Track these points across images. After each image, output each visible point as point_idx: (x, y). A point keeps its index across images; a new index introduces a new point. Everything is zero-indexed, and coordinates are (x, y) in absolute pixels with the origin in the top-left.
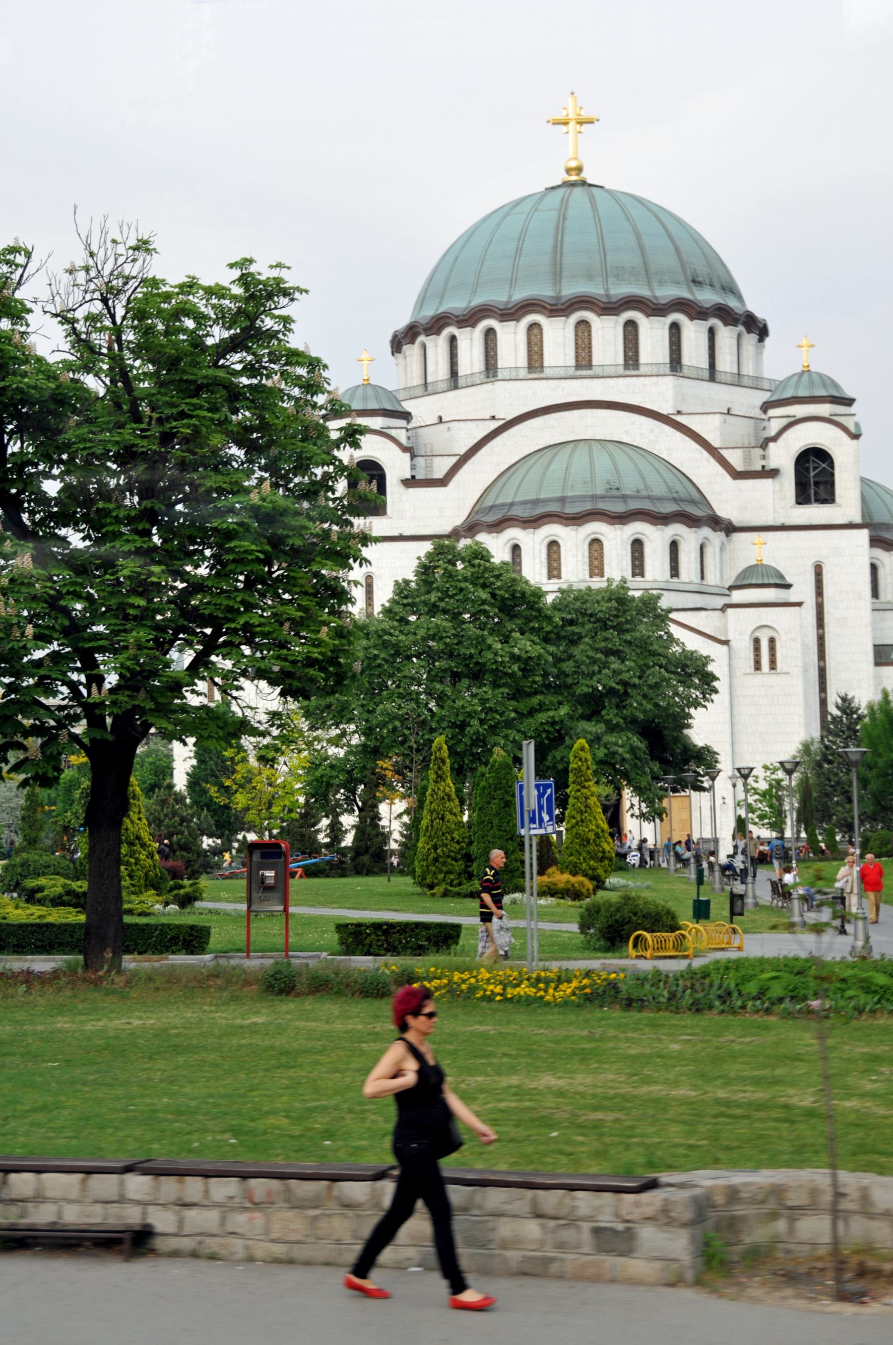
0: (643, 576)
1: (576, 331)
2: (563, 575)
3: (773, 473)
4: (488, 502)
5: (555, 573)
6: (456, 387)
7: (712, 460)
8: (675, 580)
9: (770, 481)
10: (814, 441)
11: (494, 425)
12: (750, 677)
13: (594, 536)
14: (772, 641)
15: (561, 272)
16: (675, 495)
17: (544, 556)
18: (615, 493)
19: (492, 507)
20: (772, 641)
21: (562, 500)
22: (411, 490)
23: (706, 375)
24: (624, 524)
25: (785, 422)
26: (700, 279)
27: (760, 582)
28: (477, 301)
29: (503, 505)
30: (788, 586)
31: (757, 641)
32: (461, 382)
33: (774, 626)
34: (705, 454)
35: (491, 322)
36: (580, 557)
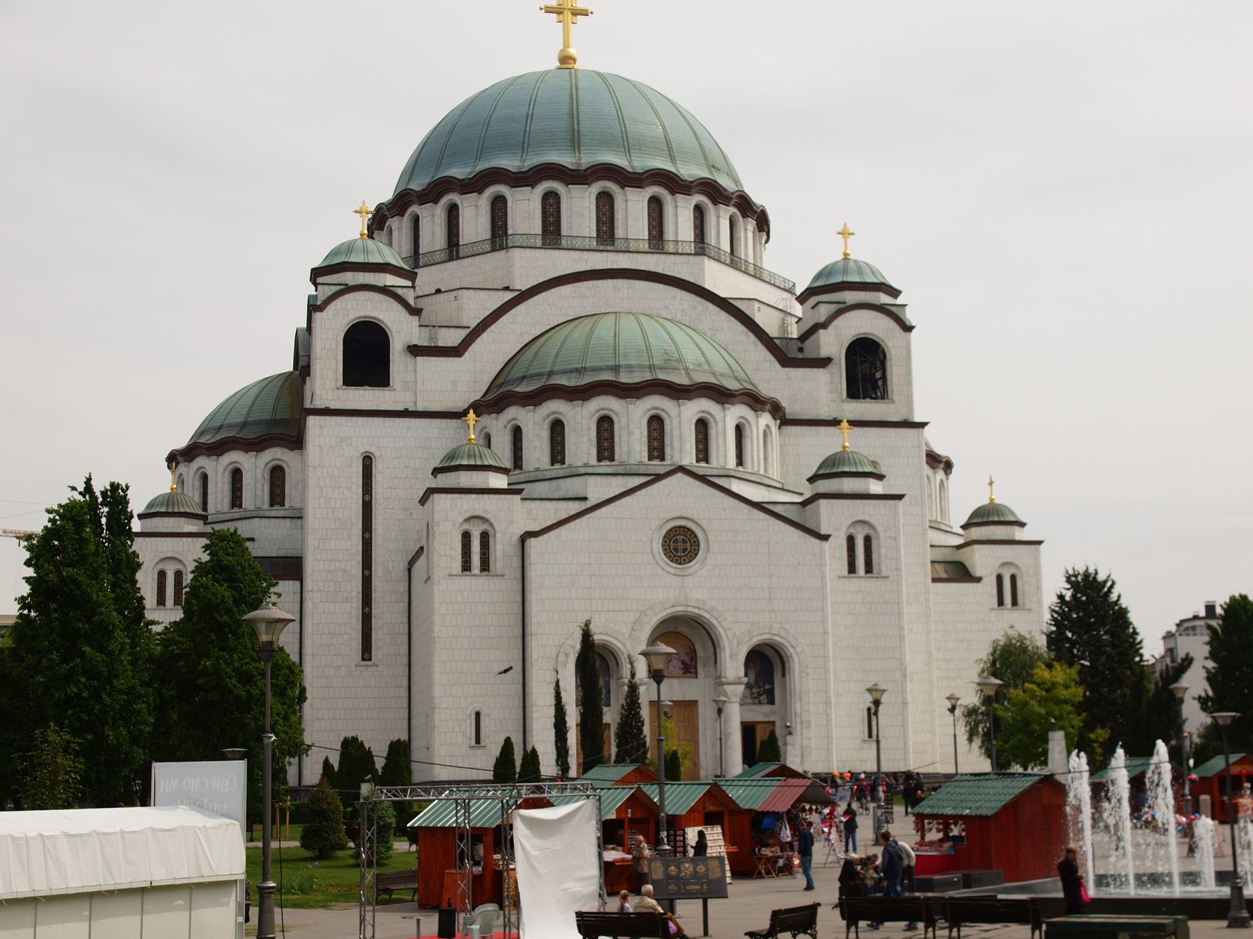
0: (707, 460)
1: (597, 203)
2: (617, 457)
3: (824, 362)
4: (518, 371)
5: (606, 454)
6: (458, 258)
7: (759, 344)
8: (740, 468)
10: (866, 331)
11: (508, 296)
13: (654, 412)
14: (868, 540)
16: (736, 373)
17: (594, 433)
18: (674, 364)
19: (524, 377)
20: (868, 540)
22: (418, 358)
24: (689, 399)
25: (834, 308)
26: (720, 167)
27: (853, 470)
28: (482, 166)
29: (540, 375)
30: (880, 477)
33: (873, 521)
34: (752, 337)
35: (501, 189)
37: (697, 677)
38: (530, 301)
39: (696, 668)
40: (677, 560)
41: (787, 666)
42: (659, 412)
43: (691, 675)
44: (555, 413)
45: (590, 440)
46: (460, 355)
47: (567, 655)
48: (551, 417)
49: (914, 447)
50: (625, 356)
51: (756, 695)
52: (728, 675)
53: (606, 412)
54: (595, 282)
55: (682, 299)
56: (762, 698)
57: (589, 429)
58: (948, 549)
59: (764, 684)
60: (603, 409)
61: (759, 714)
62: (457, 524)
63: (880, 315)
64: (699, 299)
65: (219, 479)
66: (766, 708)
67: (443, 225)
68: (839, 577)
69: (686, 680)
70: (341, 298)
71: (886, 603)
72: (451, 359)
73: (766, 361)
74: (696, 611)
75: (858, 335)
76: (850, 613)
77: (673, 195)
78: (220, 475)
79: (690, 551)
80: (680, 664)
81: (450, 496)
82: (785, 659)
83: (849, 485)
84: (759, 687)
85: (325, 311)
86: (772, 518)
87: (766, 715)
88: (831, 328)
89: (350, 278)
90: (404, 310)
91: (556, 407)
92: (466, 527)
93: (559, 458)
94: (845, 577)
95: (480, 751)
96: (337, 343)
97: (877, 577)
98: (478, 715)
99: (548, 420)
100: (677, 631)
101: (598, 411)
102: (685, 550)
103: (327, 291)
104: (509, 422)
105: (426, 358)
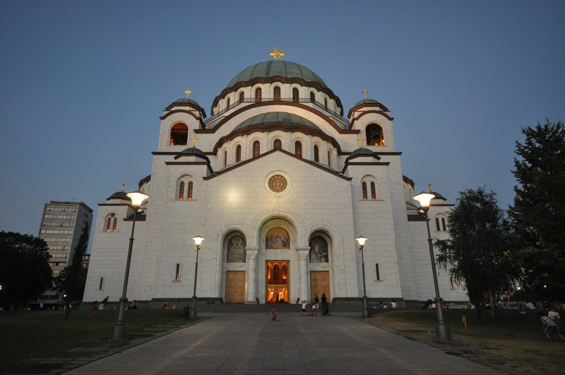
3: (357, 132)
8: (317, 163)
9: (356, 134)
12: (362, 202)
13: (276, 138)
14: (373, 184)
15: (269, 72)
17: (252, 148)
20: (373, 184)
21: (263, 123)
22: (198, 134)
23: (324, 108)
25: (361, 113)
31: (364, 184)
32: (230, 107)
33: (374, 175)
34: (328, 123)
37: (289, 249)
38: (241, 114)
39: (289, 245)
40: (276, 191)
41: (332, 242)
42: (279, 138)
43: (286, 248)
44: (238, 142)
45: (250, 150)
46: (214, 133)
47: (218, 235)
48: (237, 144)
49: (396, 162)
50: (267, 119)
51: (319, 258)
53: (257, 139)
54: (266, 106)
55: (300, 111)
56: (322, 259)
57: (250, 146)
58: (414, 210)
59: (323, 252)
60: (256, 138)
61: (320, 266)
62: (177, 178)
63: (379, 115)
64: (306, 111)
65: (146, 191)
66: (324, 264)
67: (225, 105)
68: (359, 200)
69: (284, 250)
70: (172, 115)
71: (383, 213)
72: (210, 134)
73: (333, 132)
74: (285, 214)
75: (370, 122)
76: (365, 218)
77: (302, 87)
78: (146, 189)
79: (283, 186)
80: (281, 242)
81: (175, 166)
82: (331, 238)
84: (321, 254)
85: (165, 119)
86: (323, 171)
87: (324, 268)
88: (359, 120)
89: (175, 108)
90: (194, 118)
91: (239, 140)
92: (182, 179)
93: (239, 160)
94: (362, 200)
95: (178, 284)
96: (169, 130)
97: (378, 200)
98: (178, 265)
99: (236, 146)
100: (280, 227)
101: (253, 139)
102: (280, 186)
103: (167, 112)
104: (223, 150)
105: (201, 134)
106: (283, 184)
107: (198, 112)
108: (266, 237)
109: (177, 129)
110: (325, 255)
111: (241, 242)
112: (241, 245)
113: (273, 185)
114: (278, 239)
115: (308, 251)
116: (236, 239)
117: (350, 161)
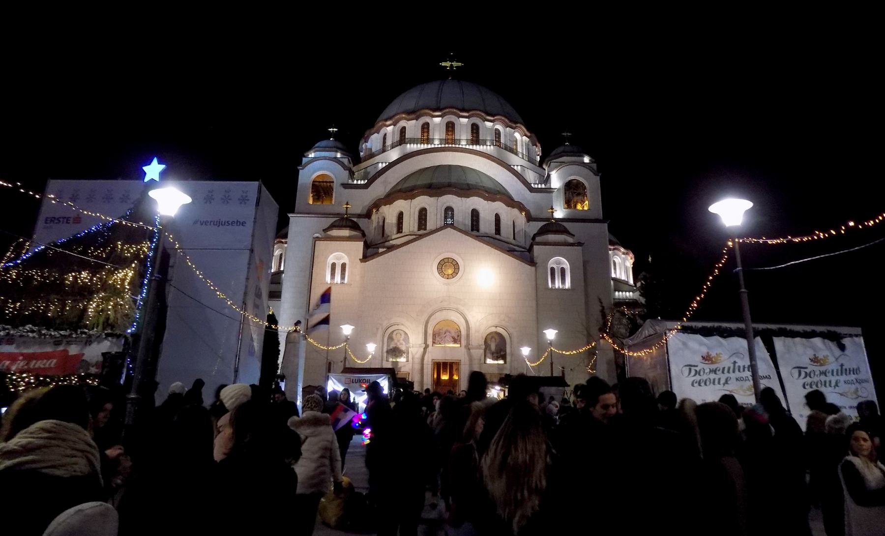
0: (478, 230)
30: (573, 235)
36: (439, 216)
39: (460, 341)
47: (377, 329)
51: (495, 357)
52: (473, 344)
64: (488, 160)
80: (451, 338)
83: (551, 237)
86: (502, 253)
91: (400, 205)
93: (401, 230)
106: (455, 269)
107: (347, 159)
108: (433, 331)
109: (320, 182)
110: (502, 355)
111: (403, 336)
112: (403, 340)
113: (443, 269)
114: (448, 333)
115: (482, 351)
116: (397, 334)
117: (538, 239)
